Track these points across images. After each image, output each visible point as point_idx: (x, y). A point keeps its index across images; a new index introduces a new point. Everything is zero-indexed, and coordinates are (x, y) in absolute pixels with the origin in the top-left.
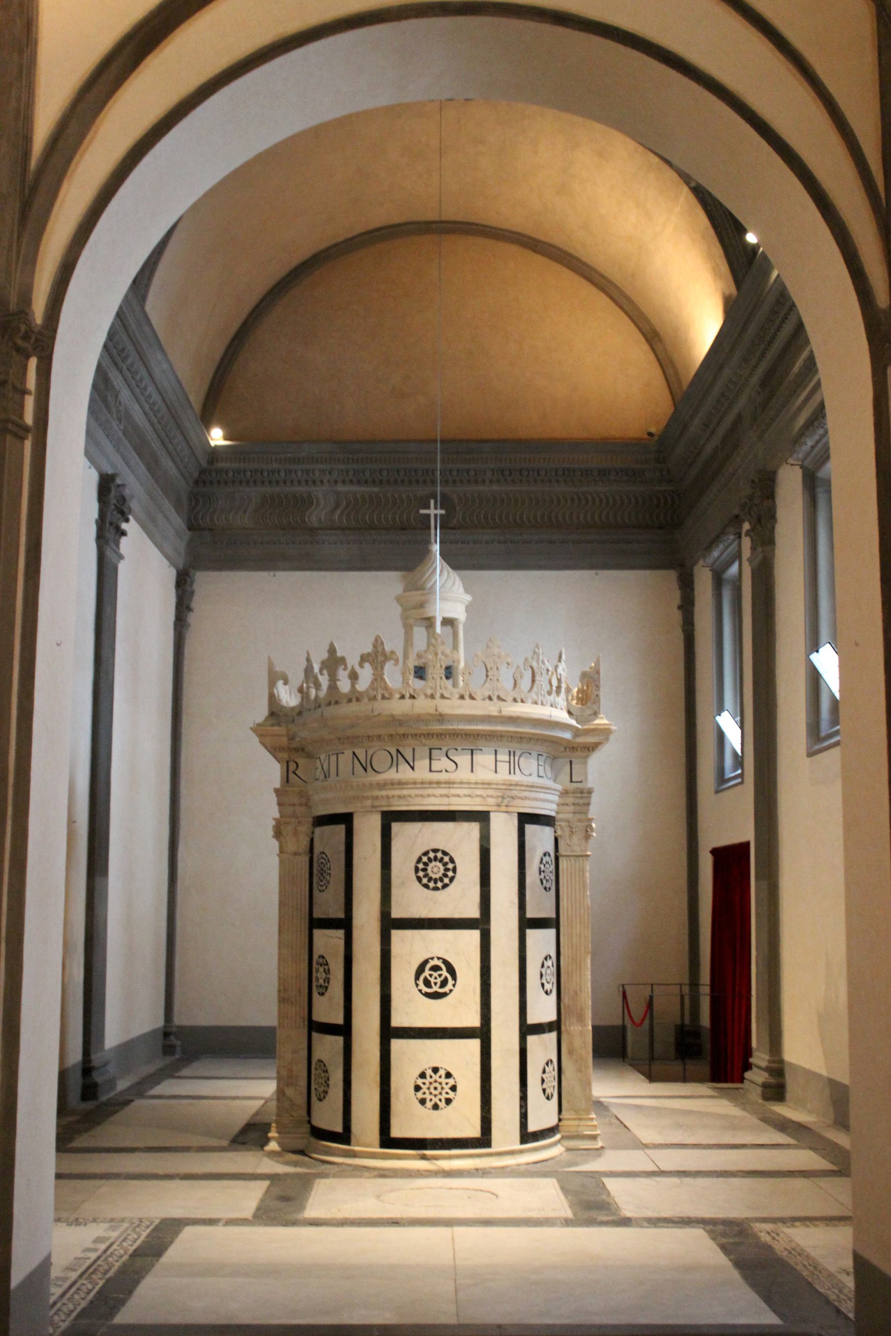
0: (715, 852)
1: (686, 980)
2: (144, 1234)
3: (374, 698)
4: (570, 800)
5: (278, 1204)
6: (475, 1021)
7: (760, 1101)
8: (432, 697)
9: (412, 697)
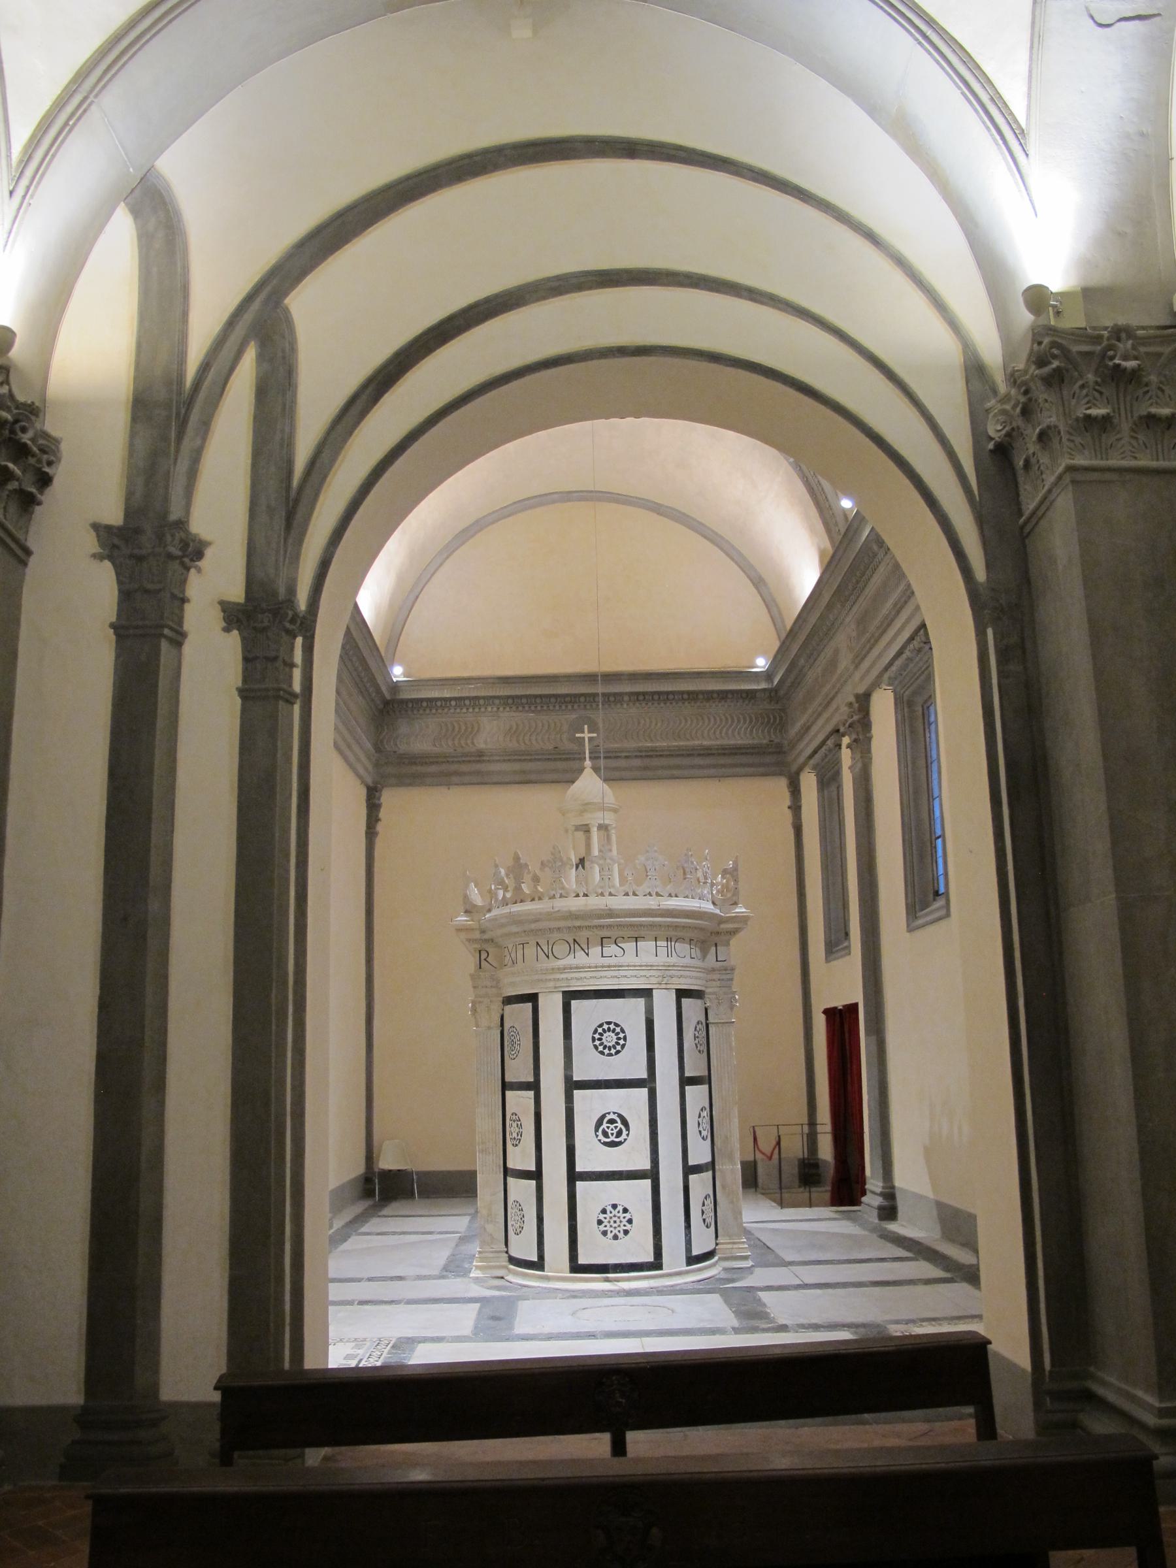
0: (827, 1012)
1: (805, 1120)
2: (386, 1351)
3: (554, 897)
4: (716, 976)
5: (492, 1323)
6: (647, 1165)
7: (877, 1221)
8: (602, 894)
9: (586, 895)
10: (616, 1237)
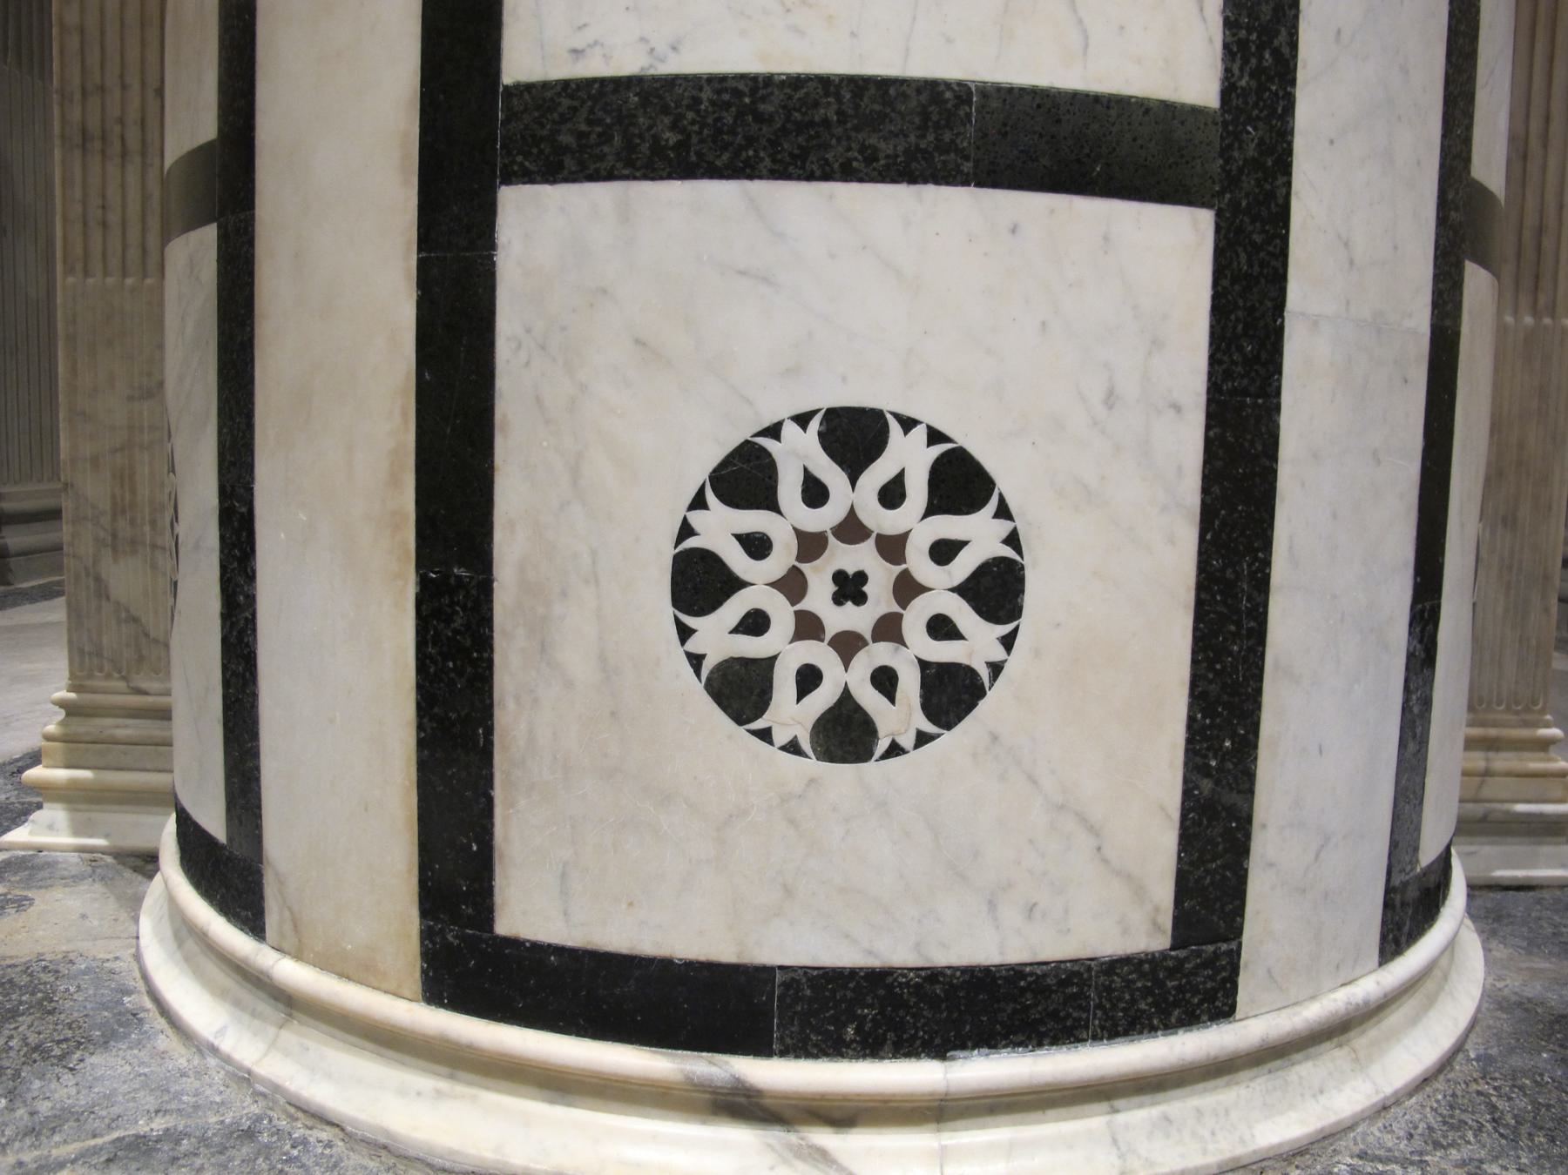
10: (846, 736)
